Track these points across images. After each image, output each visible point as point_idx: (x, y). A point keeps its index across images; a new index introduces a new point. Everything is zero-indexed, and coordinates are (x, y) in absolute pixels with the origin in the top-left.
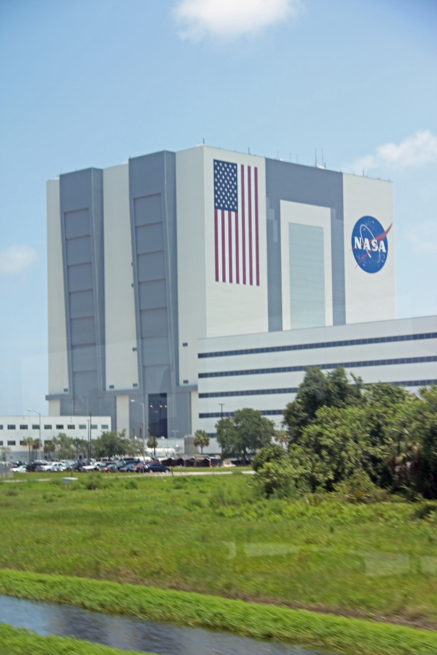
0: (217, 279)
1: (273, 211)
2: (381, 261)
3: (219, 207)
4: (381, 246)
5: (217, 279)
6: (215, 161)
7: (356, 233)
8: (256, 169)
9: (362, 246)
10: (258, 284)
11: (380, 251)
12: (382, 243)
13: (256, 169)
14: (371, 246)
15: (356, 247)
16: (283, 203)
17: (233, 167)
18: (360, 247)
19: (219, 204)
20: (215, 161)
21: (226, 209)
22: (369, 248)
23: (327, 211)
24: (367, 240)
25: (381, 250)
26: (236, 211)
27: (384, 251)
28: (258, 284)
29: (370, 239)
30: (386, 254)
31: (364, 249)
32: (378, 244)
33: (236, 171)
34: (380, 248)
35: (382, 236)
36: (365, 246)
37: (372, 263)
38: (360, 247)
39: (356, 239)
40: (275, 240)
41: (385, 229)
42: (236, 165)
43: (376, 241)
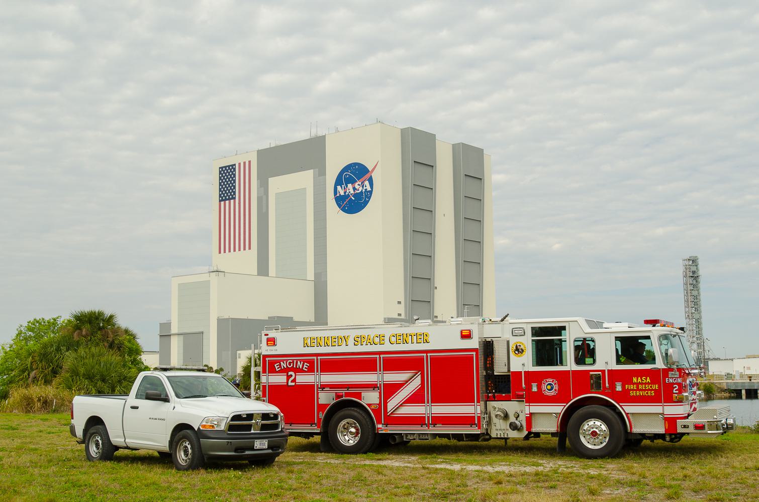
0: (220, 253)
1: (263, 188)
2: (365, 199)
3: (222, 200)
4: (366, 186)
5: (220, 253)
6: (220, 168)
8: (250, 162)
9: (345, 193)
10: (250, 248)
11: (364, 191)
12: (367, 183)
13: (250, 162)
14: (354, 189)
15: (338, 195)
16: (272, 181)
17: (233, 168)
18: (342, 193)
19: (222, 198)
20: (220, 168)
21: (227, 200)
22: (352, 192)
23: (310, 174)
24: (350, 186)
25: (366, 190)
26: (235, 198)
27: (369, 189)
28: (250, 248)
29: (353, 182)
30: (371, 192)
31: (347, 193)
33: (235, 170)
34: (365, 188)
35: (368, 176)
36: (348, 191)
37: (353, 204)
38: (342, 193)
40: (264, 211)
41: (370, 170)
42: (235, 165)
43: (360, 183)
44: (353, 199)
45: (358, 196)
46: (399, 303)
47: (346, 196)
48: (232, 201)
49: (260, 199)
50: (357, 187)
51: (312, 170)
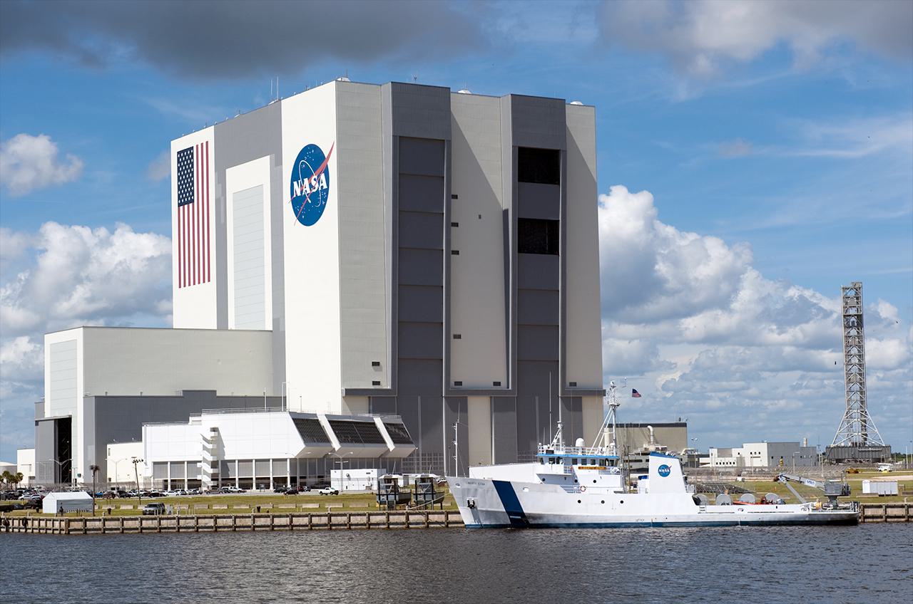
0: (180, 287)
1: (220, 185)
5: (180, 287)
7: (295, 178)
8: (207, 142)
10: (209, 281)
11: (320, 189)
12: (323, 177)
13: (207, 142)
15: (295, 196)
16: (228, 171)
18: (299, 194)
20: (178, 153)
22: (309, 192)
24: (306, 180)
25: (322, 187)
26: (192, 201)
27: (325, 187)
28: (209, 281)
29: (309, 176)
32: (319, 181)
33: (192, 154)
34: (321, 185)
35: (322, 167)
38: (299, 194)
39: (295, 183)
40: (222, 221)
43: (316, 177)
44: (310, 202)
45: (314, 196)
46: (376, 364)
47: (303, 198)
48: (191, 205)
49: (217, 201)
50: (313, 183)
51: (269, 156)
